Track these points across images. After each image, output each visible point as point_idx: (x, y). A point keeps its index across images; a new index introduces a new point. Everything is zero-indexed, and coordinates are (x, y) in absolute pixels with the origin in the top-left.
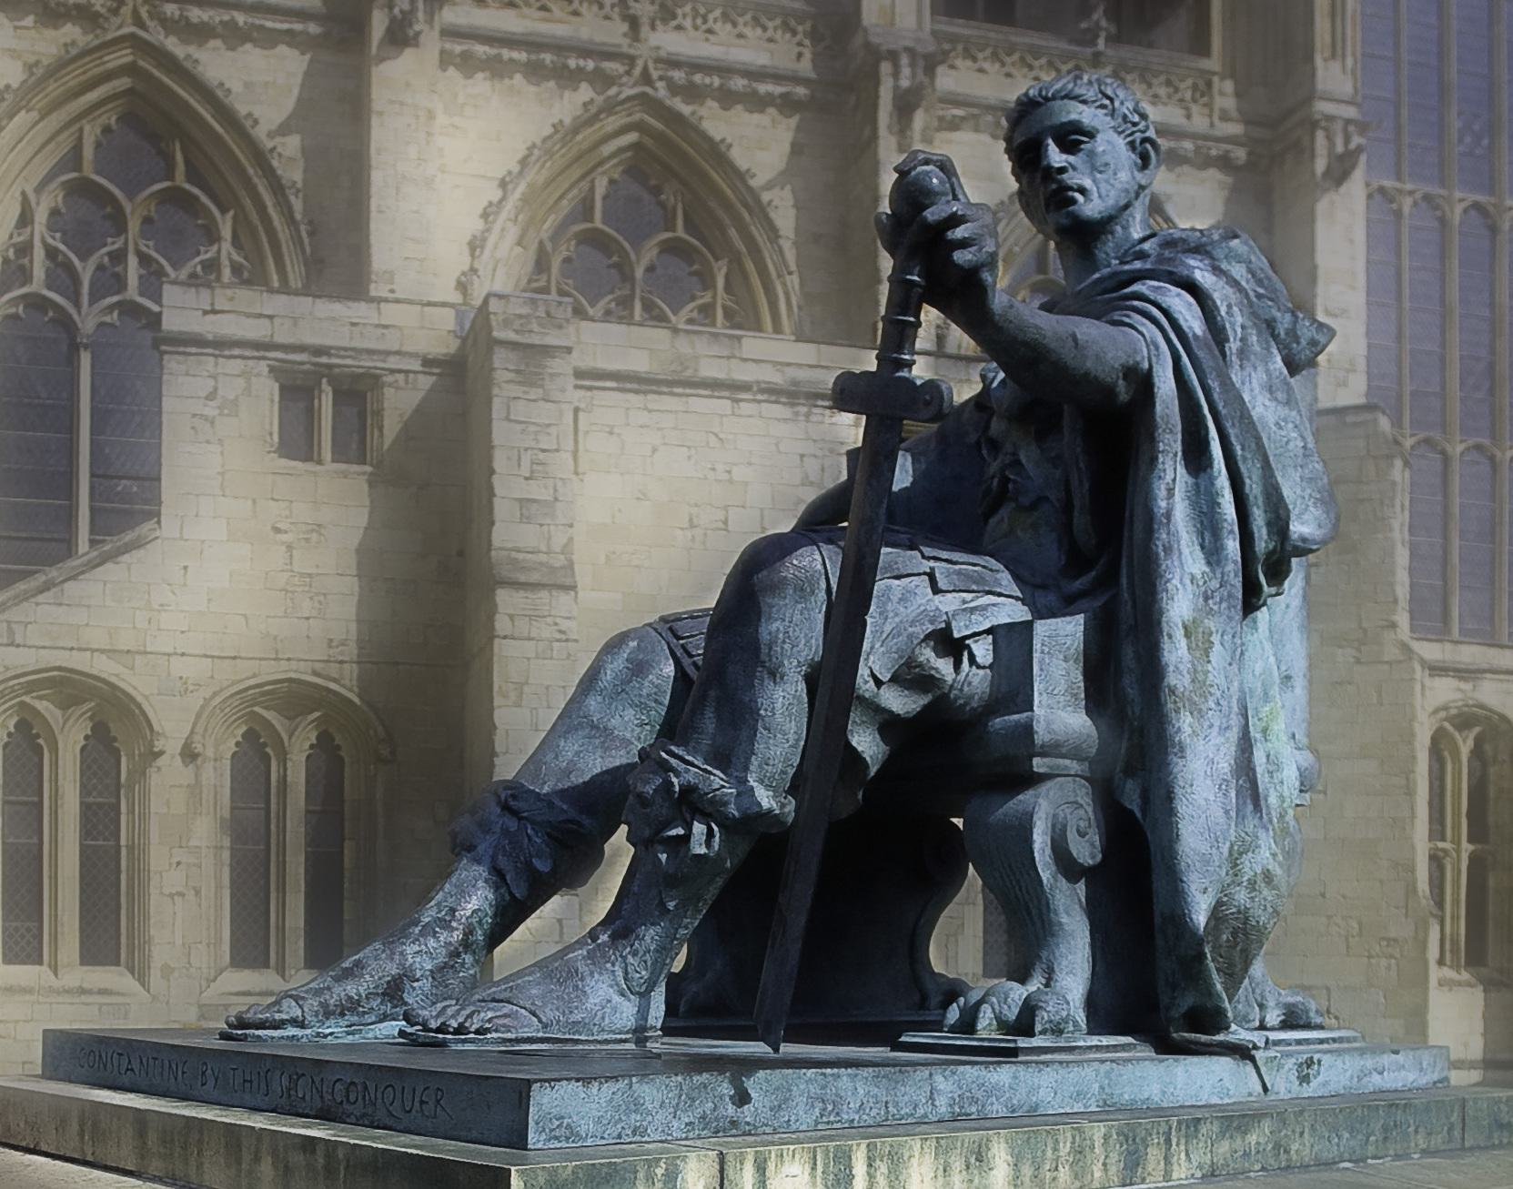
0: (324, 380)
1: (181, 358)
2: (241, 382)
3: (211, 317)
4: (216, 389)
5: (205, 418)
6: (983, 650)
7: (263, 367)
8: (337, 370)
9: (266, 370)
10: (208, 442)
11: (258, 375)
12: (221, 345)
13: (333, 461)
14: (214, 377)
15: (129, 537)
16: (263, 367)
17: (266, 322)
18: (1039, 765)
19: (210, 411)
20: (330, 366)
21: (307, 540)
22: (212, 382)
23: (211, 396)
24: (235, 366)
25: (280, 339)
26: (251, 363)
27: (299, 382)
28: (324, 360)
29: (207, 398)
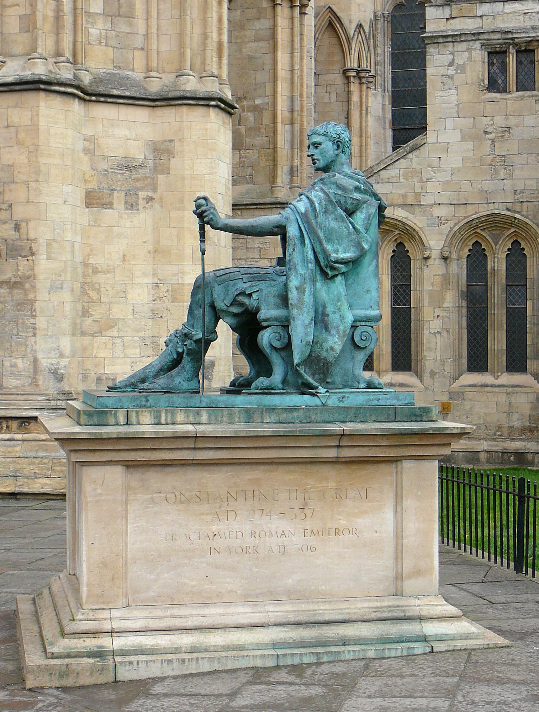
0: (511, 47)
1: (435, 45)
2: (466, 54)
3: (451, 21)
4: (453, 60)
5: (451, 77)
6: (255, 296)
7: (478, 44)
8: (516, 40)
9: (480, 45)
10: (450, 89)
11: (475, 49)
12: (456, 38)
13: (517, 91)
14: (452, 54)
15: (411, 143)
16: (478, 44)
17: (479, 20)
18: (264, 324)
19: (451, 72)
20: (512, 39)
21: (502, 137)
22: (451, 57)
23: (451, 64)
24: (464, 46)
25: (486, 28)
26: (471, 43)
27: (498, 49)
28: (510, 36)
29: (449, 66)
